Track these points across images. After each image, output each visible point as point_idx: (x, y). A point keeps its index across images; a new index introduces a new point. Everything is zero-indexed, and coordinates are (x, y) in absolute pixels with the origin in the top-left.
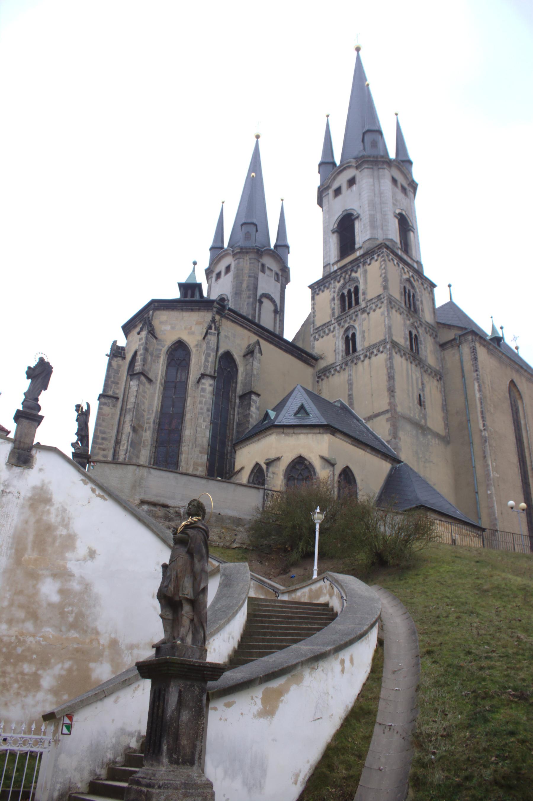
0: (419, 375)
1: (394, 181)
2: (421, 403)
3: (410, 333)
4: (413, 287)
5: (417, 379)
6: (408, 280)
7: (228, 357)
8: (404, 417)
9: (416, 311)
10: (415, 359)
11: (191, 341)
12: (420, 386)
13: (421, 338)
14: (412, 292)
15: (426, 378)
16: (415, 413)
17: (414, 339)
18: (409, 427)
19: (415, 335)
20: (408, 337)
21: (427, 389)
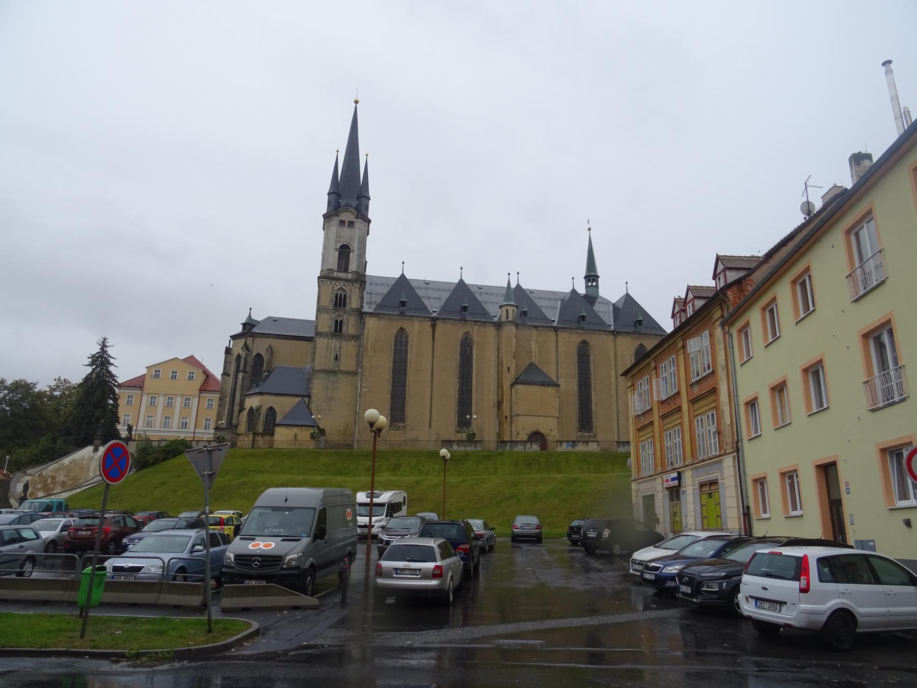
0: (338, 344)
1: (342, 222)
2: (336, 358)
3: (336, 321)
4: (345, 291)
5: (335, 347)
6: (341, 288)
7: (259, 355)
8: (319, 371)
9: (345, 305)
10: (334, 336)
11: (241, 352)
12: (338, 349)
13: (345, 321)
14: (343, 294)
15: (344, 343)
16: (331, 365)
17: (338, 326)
18: (321, 375)
19: (341, 321)
20: (333, 325)
21: (345, 349)
